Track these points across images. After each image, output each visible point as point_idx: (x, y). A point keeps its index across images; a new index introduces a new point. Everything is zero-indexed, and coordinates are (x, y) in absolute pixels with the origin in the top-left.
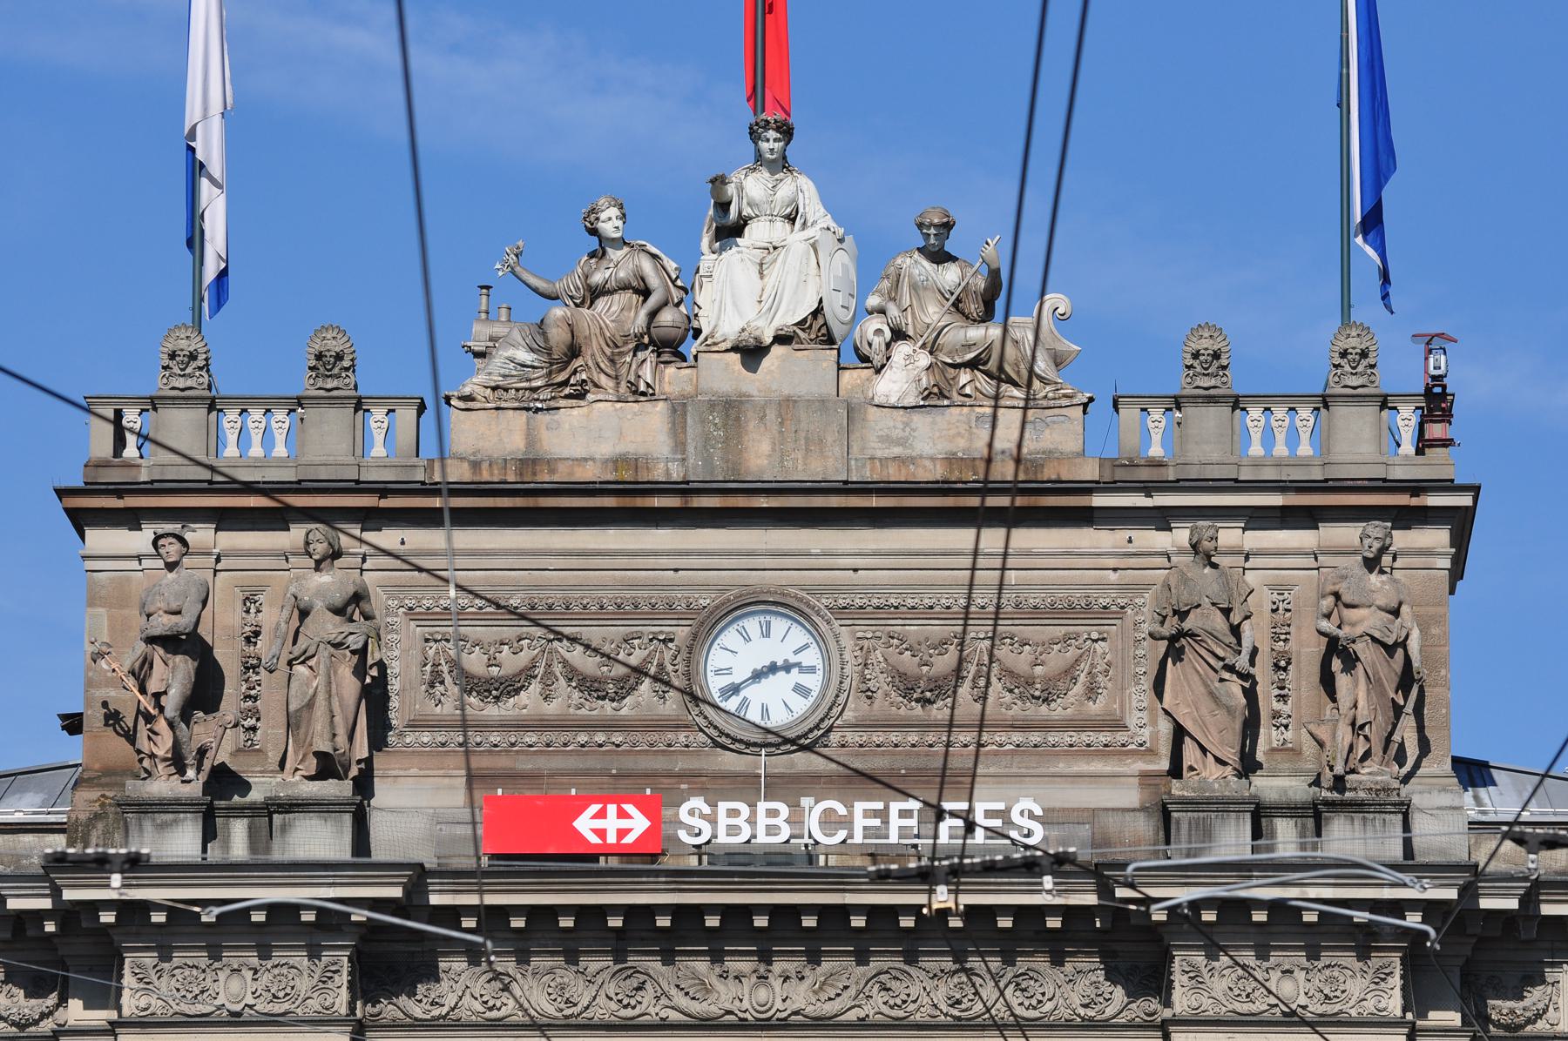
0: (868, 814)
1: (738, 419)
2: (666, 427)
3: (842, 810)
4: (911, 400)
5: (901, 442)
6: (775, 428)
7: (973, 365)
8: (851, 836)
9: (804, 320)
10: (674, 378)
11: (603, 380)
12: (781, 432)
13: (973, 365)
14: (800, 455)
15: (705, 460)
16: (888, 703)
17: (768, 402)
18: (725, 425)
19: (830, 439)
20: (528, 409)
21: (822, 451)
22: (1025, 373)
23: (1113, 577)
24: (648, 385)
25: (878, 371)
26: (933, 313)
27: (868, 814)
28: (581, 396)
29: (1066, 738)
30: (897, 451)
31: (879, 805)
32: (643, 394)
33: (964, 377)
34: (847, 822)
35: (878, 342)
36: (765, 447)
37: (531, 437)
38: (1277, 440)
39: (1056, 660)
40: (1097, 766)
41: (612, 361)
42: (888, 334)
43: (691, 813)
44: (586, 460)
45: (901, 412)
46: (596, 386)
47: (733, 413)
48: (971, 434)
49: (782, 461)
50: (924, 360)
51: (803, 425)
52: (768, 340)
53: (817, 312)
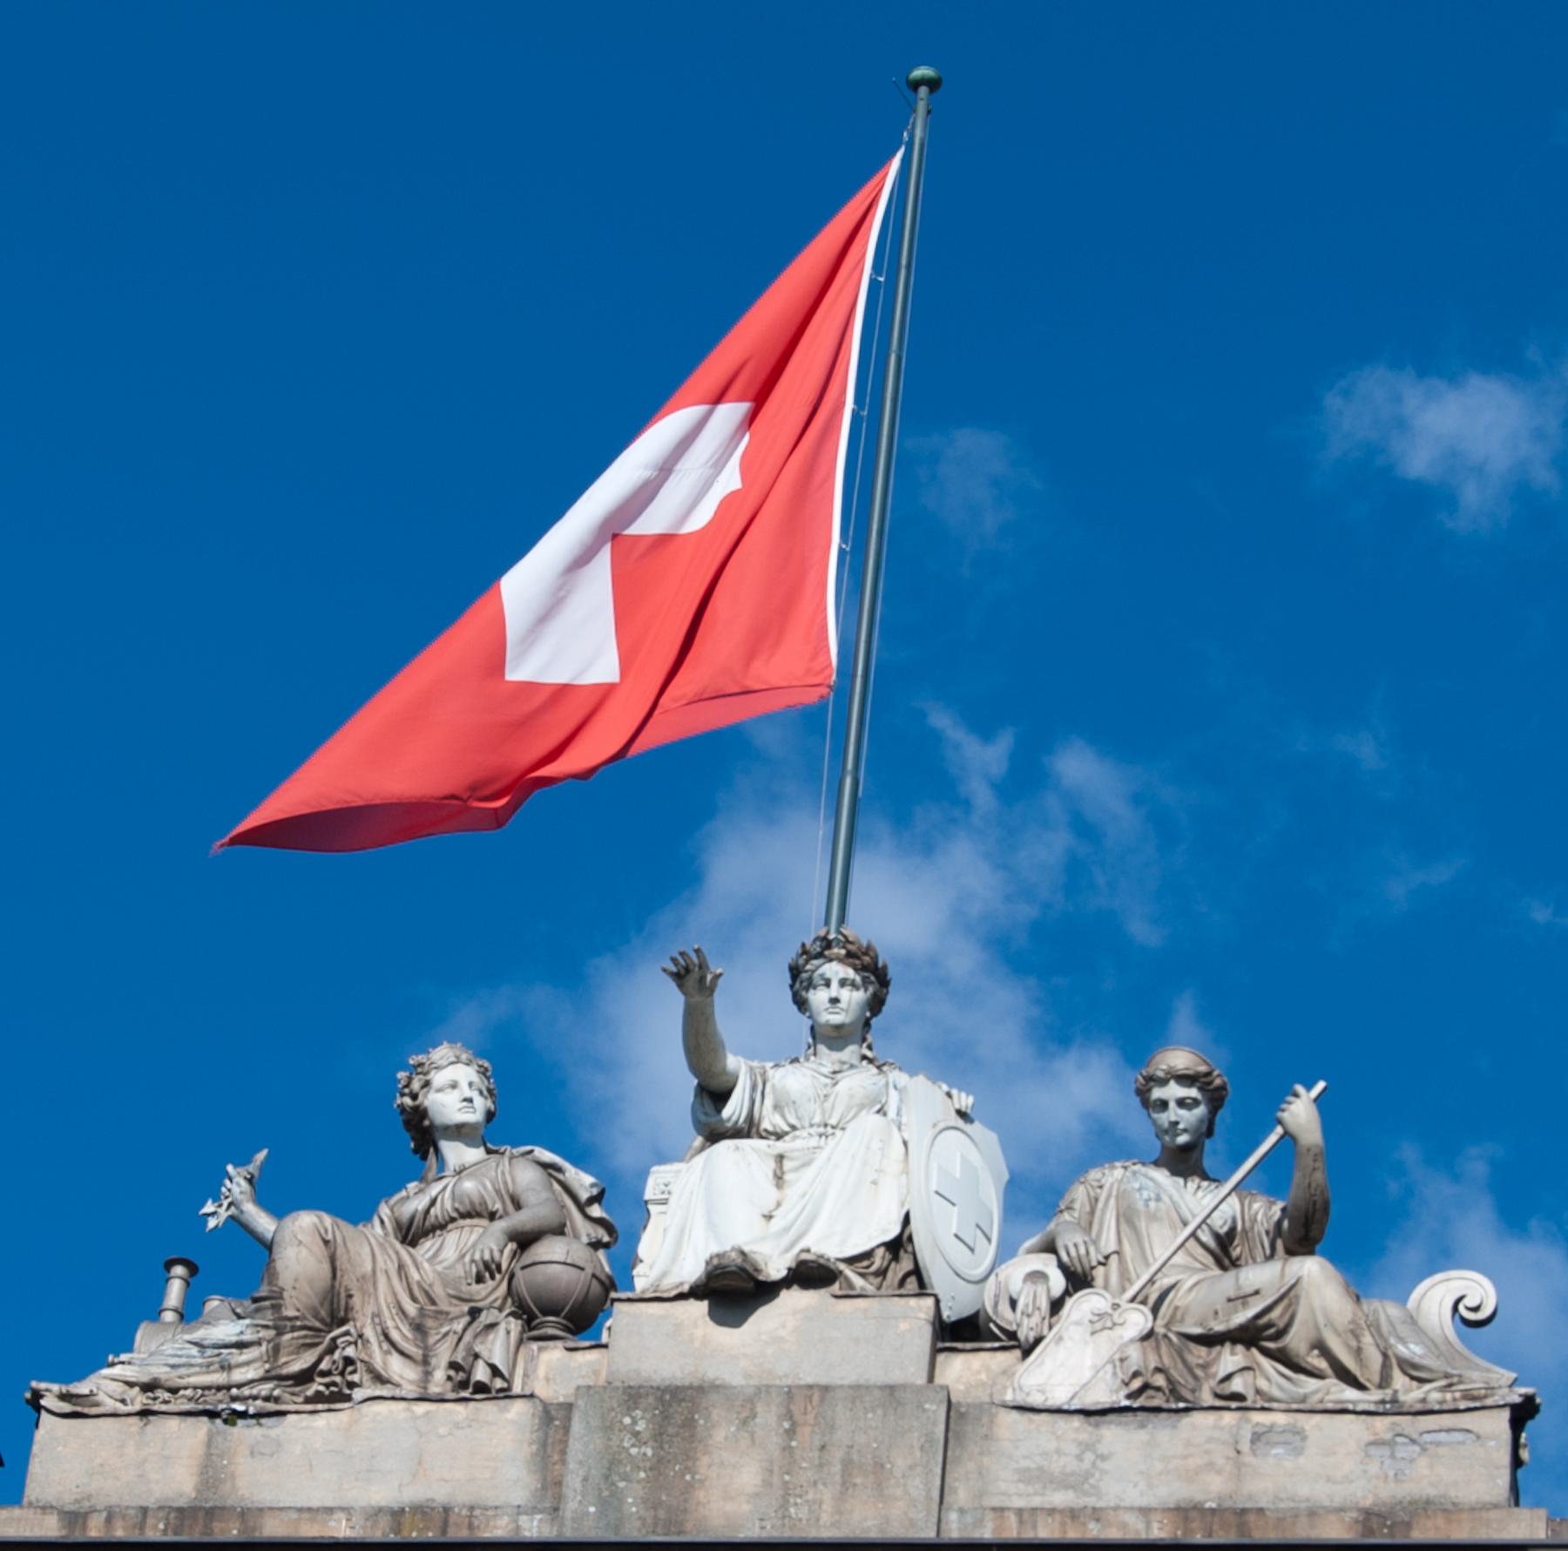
1: (690, 1423)
2: (528, 1450)
4: (1105, 1394)
6: (774, 1441)
7: (1249, 1336)
9: (868, 1255)
10: (555, 1368)
11: (397, 1367)
12: (787, 1449)
13: (1249, 1336)
14: (827, 1495)
15: (603, 1504)
17: (763, 1391)
18: (658, 1437)
19: (900, 1462)
20: (212, 1415)
21: (879, 1485)
22: (1375, 1360)
24: (495, 1371)
25: (1027, 1352)
26: (1162, 1242)
28: (336, 1397)
30: (1061, 1498)
32: (481, 1388)
33: (1230, 1359)
35: (1034, 1299)
37: (211, 1469)
41: (419, 1328)
42: (1058, 1282)
44: (330, 1510)
45: (1077, 1421)
46: (380, 1379)
47: (679, 1412)
48: (1239, 1466)
49: (784, 1505)
50: (1137, 1320)
51: (842, 1435)
52: (776, 1269)
53: (898, 1246)
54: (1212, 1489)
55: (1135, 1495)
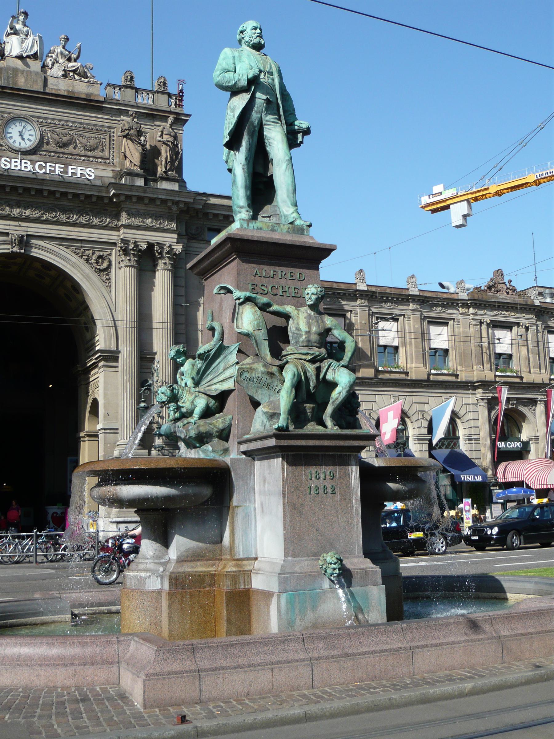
0: (50, 166)
3: (44, 165)
5: (56, 85)
8: (46, 171)
16: (52, 147)
23: (106, 124)
27: (50, 166)
29: (95, 160)
30: (55, 87)
31: (54, 165)
34: (45, 168)
36: (23, 80)
38: (145, 100)
39: (92, 142)
40: (102, 167)
43: (5, 160)
54: (70, 89)
55: (63, 88)
